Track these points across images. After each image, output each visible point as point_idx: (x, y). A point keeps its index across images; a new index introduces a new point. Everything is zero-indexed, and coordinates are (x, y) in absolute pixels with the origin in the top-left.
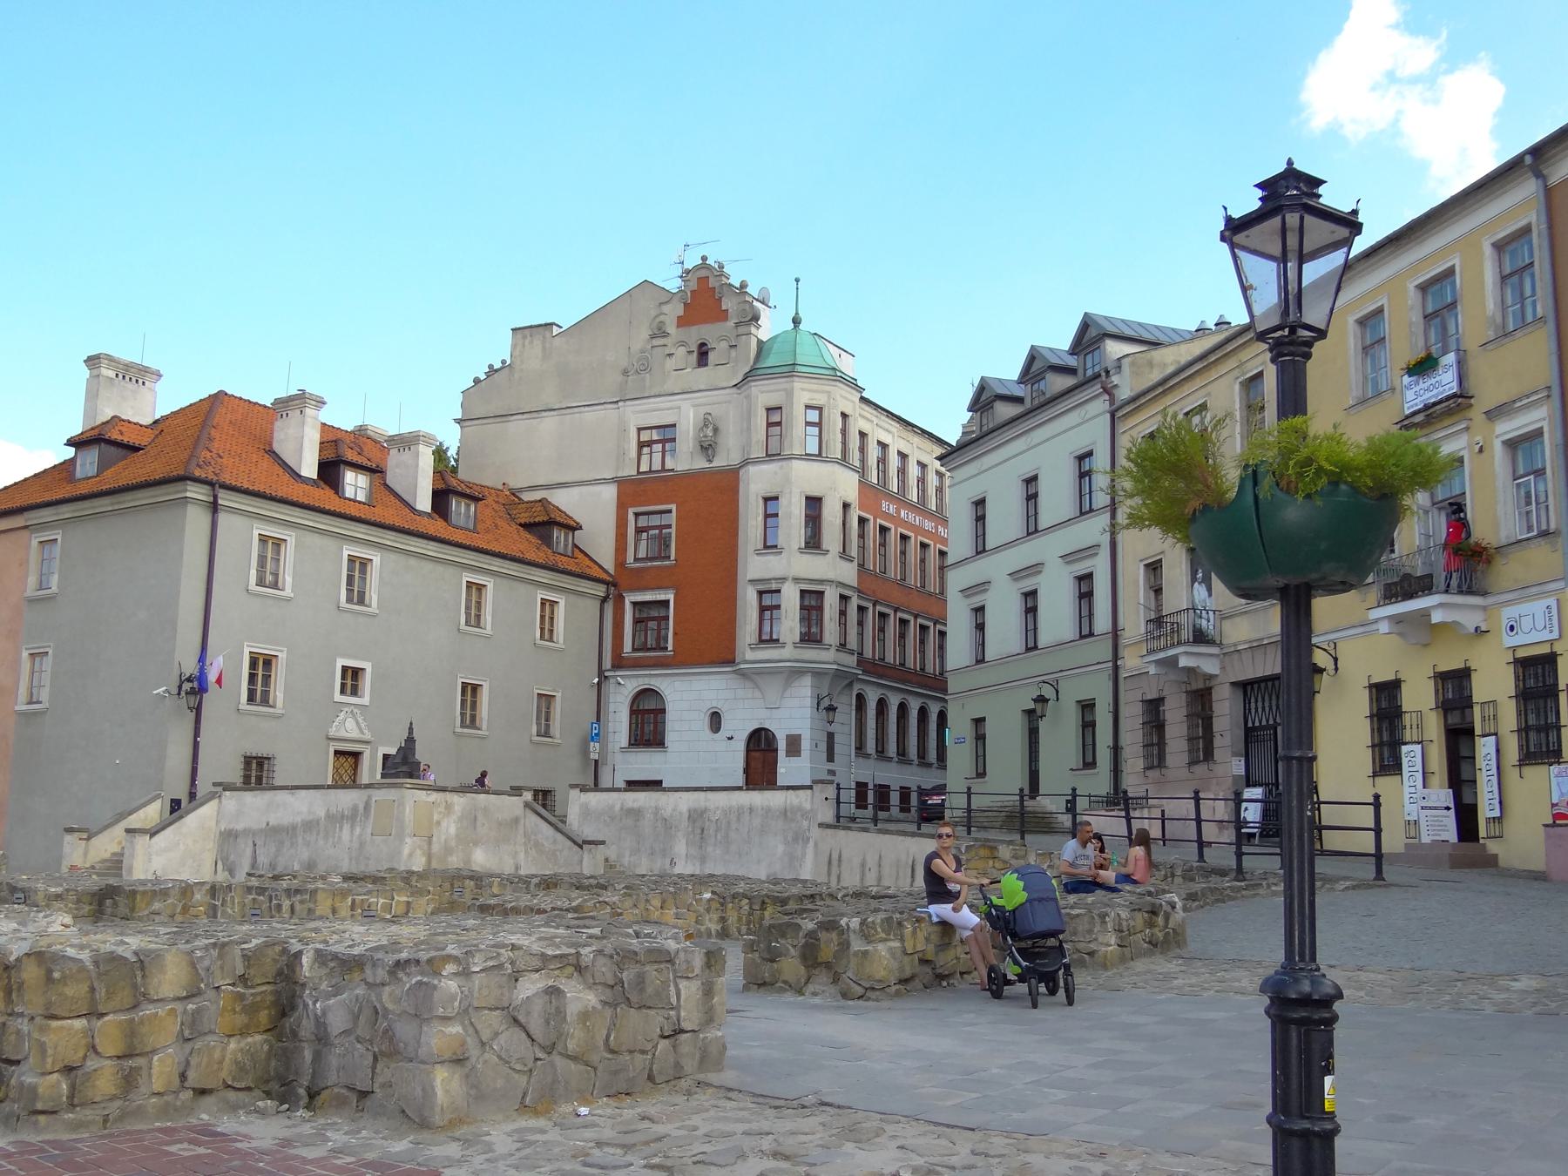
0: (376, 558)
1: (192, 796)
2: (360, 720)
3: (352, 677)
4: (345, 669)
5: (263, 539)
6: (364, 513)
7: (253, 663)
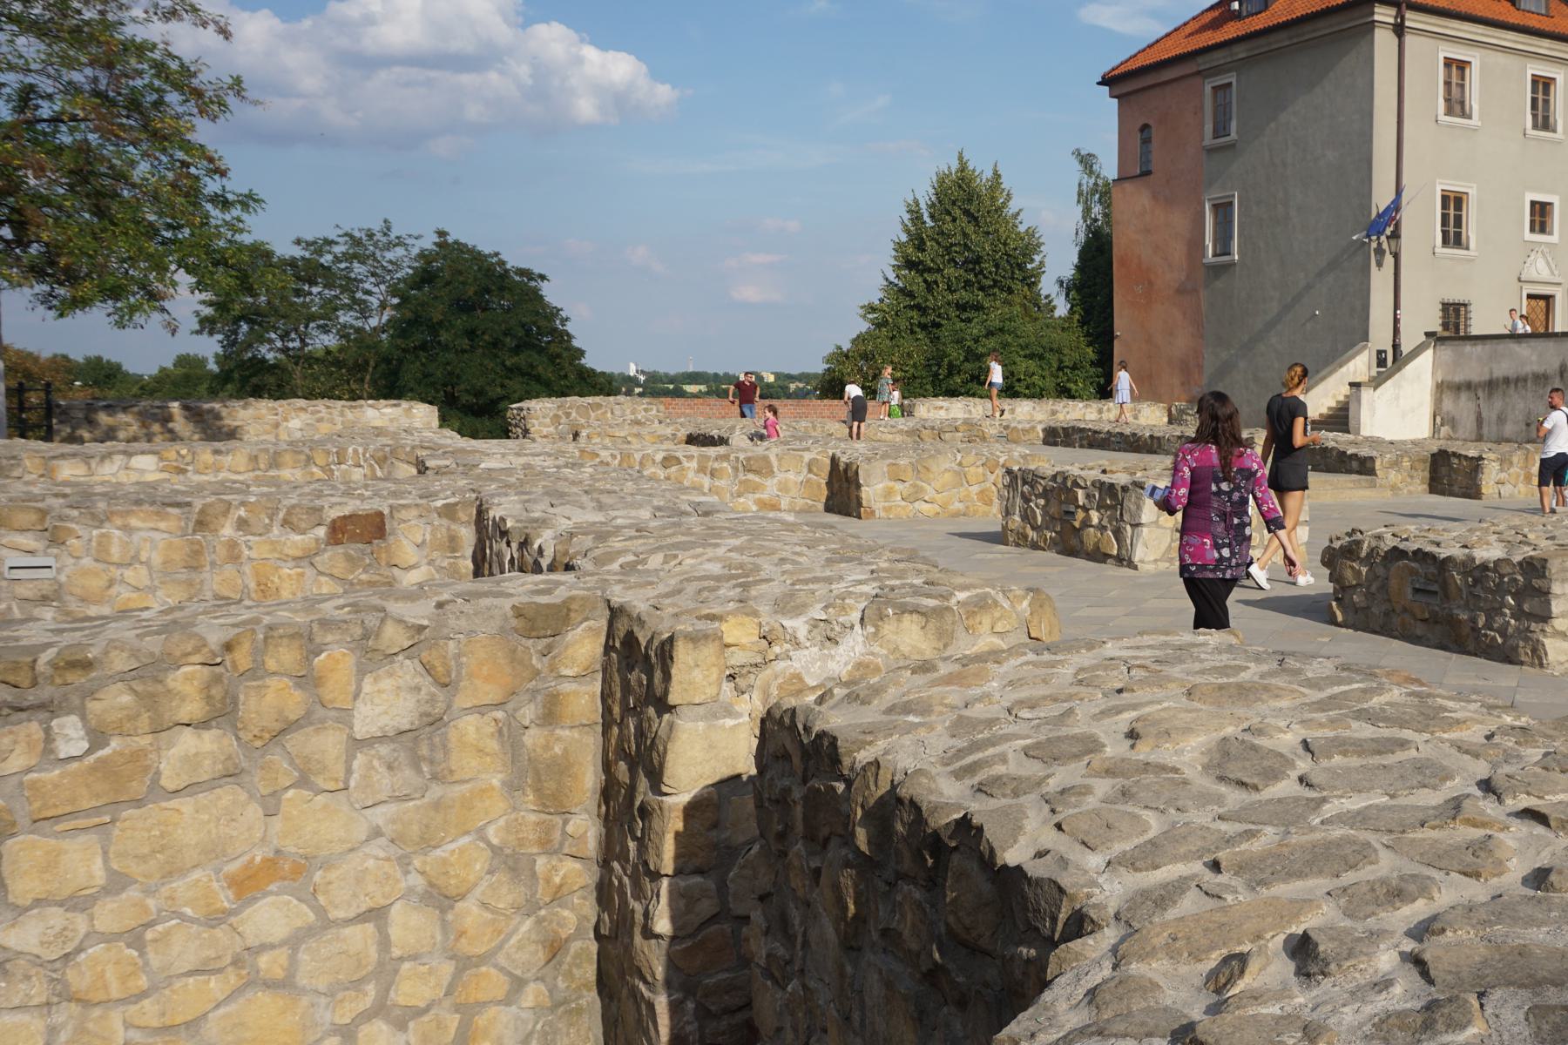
0: (1557, 73)
1: (1396, 347)
2: (1550, 259)
3: (1541, 215)
4: (1533, 203)
5: (1449, 62)
6: (1546, 25)
7: (1445, 199)
